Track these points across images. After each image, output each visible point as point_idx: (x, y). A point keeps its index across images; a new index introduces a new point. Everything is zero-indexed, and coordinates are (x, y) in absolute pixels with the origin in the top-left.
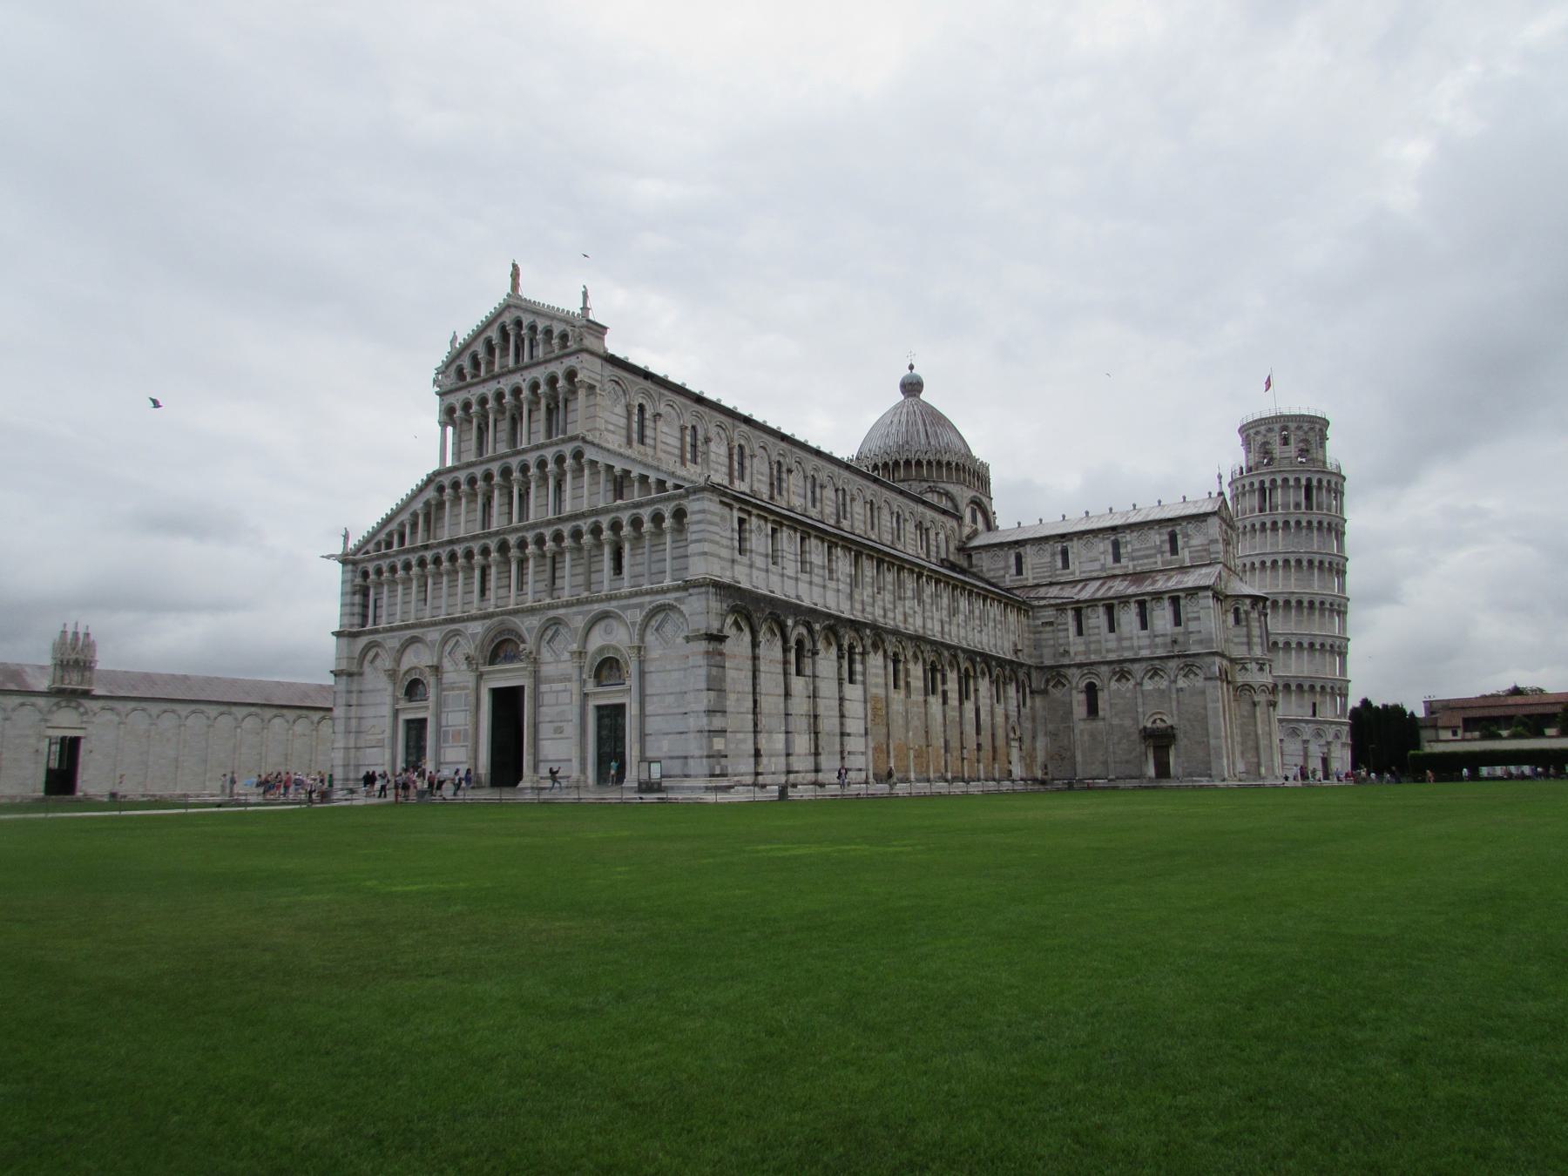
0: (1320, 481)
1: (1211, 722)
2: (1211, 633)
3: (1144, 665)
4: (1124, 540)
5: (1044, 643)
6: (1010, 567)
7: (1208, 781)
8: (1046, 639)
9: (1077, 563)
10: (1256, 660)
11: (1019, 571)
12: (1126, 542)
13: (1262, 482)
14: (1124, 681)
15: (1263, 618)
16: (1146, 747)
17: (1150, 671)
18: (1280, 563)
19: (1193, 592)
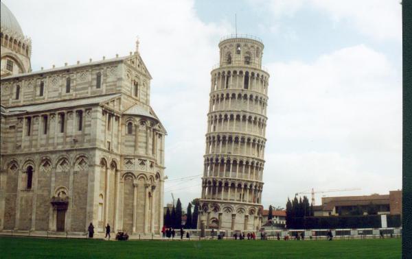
0: (253, 74)
1: (89, 195)
2: (95, 135)
3: (58, 155)
4: (73, 78)
5: (9, 140)
6: (12, 94)
7: (83, 235)
8: (10, 138)
9: (47, 92)
10: (139, 158)
11: (17, 98)
12: (74, 80)
13: (224, 72)
14: (48, 166)
15: (149, 131)
16: (54, 210)
17: (61, 160)
18: (229, 117)
19: (89, 107)
